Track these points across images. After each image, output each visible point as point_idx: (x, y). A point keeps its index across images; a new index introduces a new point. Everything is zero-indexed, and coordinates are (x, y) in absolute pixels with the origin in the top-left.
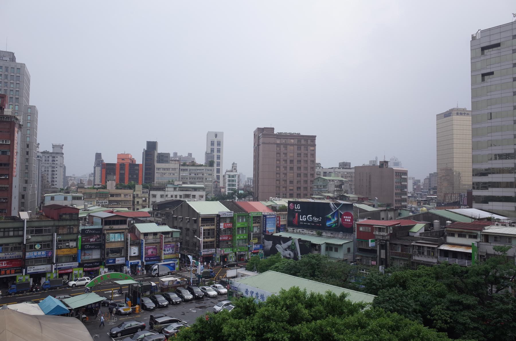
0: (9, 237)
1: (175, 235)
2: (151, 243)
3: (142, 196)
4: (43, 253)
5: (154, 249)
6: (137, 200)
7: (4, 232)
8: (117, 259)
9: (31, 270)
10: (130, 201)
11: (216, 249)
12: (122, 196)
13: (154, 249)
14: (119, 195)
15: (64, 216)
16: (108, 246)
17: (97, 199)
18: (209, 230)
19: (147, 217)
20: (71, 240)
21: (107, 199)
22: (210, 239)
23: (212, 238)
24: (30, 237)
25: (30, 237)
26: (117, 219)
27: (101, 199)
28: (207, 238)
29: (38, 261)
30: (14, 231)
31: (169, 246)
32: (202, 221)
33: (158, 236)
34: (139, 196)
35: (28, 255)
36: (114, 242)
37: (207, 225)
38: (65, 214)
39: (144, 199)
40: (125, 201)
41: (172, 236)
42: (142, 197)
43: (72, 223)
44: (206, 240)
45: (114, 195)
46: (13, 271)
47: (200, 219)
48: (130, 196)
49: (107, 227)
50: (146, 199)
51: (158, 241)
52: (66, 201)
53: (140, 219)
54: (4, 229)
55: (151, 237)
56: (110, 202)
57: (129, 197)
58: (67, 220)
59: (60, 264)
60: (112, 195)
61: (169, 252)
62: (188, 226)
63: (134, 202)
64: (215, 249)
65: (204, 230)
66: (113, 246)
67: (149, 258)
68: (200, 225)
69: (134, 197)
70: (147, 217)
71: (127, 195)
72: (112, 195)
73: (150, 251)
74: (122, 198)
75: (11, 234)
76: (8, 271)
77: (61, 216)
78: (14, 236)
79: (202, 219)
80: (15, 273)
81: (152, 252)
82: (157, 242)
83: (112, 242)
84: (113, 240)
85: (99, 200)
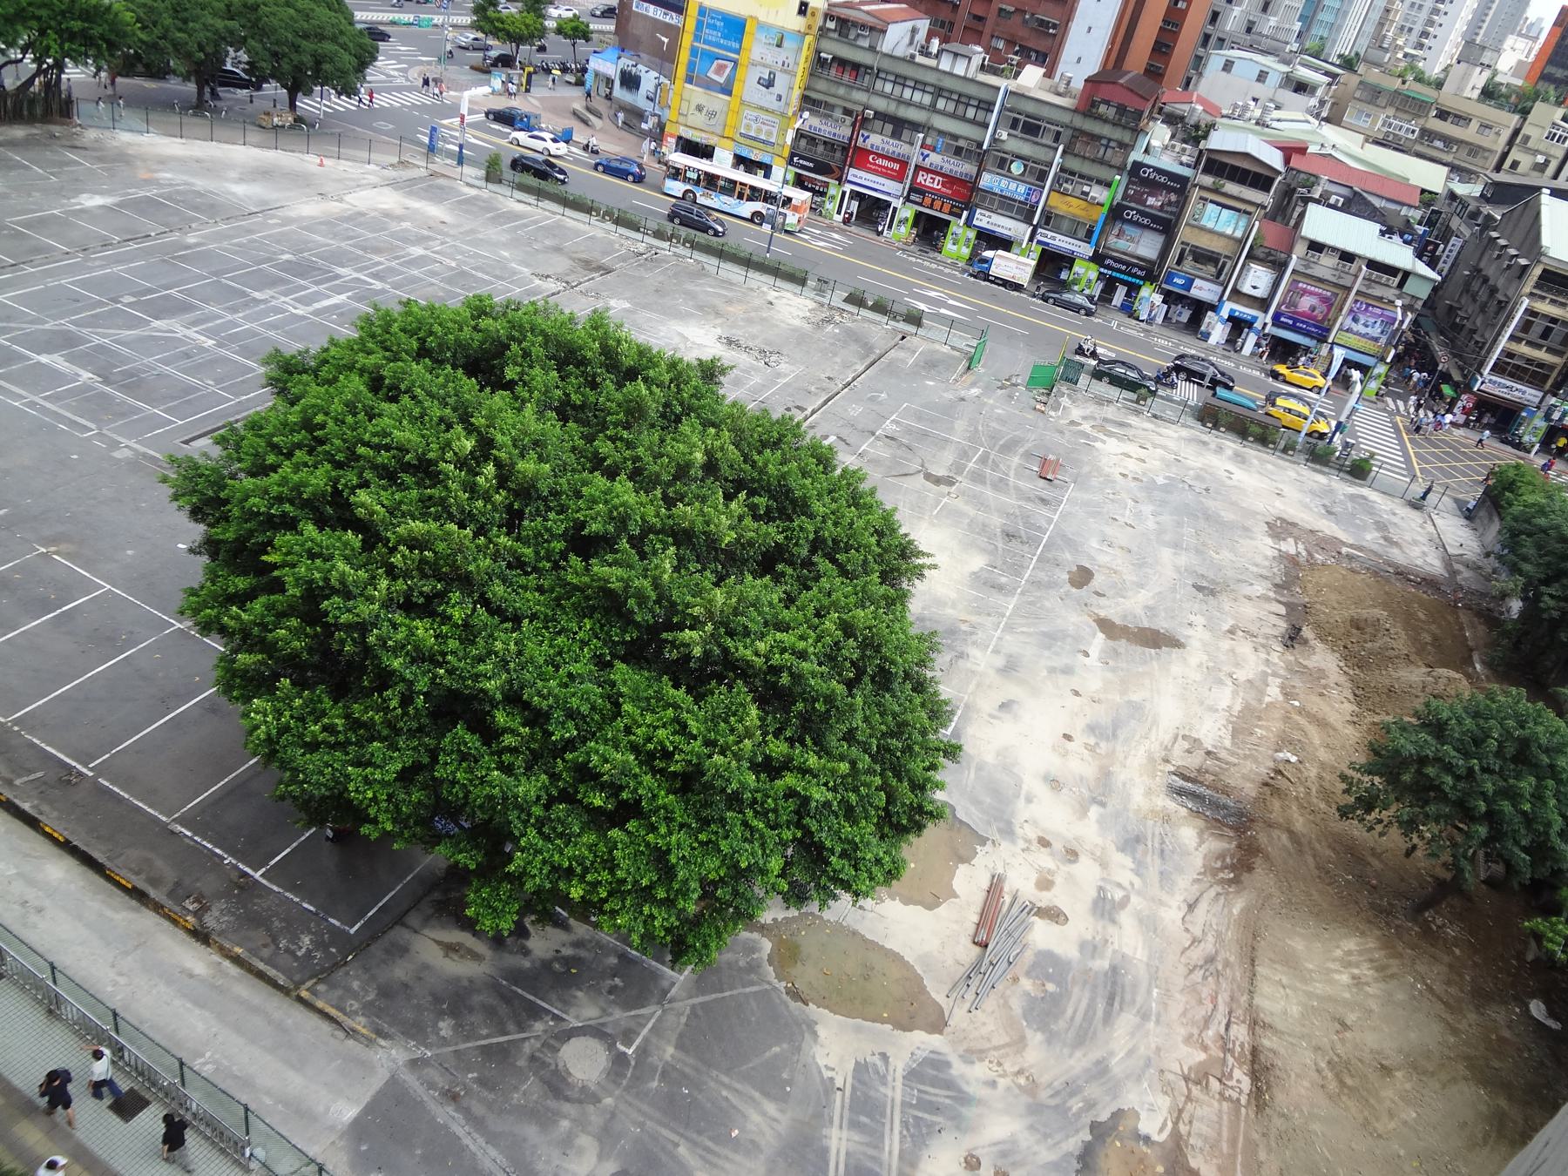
0: (963, 119)
1: (1411, 287)
2: (1321, 280)
3: (1541, 147)
4: (1022, 188)
5: (1324, 300)
6: (1515, 155)
7: (958, 102)
8: (1197, 282)
9: (984, 219)
10: (1490, 151)
11: (1546, 394)
12: (1474, 125)
13: (1324, 300)
14: (1462, 119)
15: (1102, 109)
16: (1184, 234)
17: (1391, 111)
18: (1554, 320)
19: (1403, 204)
20: (1099, 182)
21: (1421, 121)
22: (1541, 355)
23: (1550, 350)
24: (1004, 136)
25: (1004, 136)
26: (1245, 165)
27: (1400, 114)
28: (1530, 343)
29: (1005, 204)
30: (978, 107)
31: (1378, 311)
32: (1541, 277)
33: (1354, 266)
34: (1530, 144)
35: (987, 181)
36: (1211, 231)
37: (1553, 302)
38: (1107, 103)
39: (1540, 159)
40: (1475, 150)
41: (1401, 285)
42: (1536, 152)
43: (1117, 134)
44: (1523, 349)
45: (1448, 113)
46: (947, 208)
47: (1538, 271)
48: (1498, 134)
49: (1208, 180)
50: (1547, 163)
51: (1347, 281)
52: (1259, 85)
53: (1377, 203)
54: (960, 95)
55: (1327, 262)
56: (1427, 135)
57: (1492, 136)
58: (1106, 121)
59: (1050, 234)
60: (1443, 115)
61: (1369, 330)
62: (1501, 283)
63: (1504, 156)
64: (1540, 394)
65: (1530, 312)
66: (1205, 242)
67: (1296, 320)
68: (1527, 289)
69: (1511, 143)
70: (1403, 204)
71: (1490, 128)
72: (1443, 115)
73: (1306, 303)
74: (1469, 133)
75: (971, 113)
76: (928, 201)
77: (1094, 104)
78: (973, 122)
79: (1545, 271)
80: (951, 213)
81: (1313, 309)
82: (1341, 282)
83: (1203, 229)
84: (1210, 225)
85: (1395, 118)
